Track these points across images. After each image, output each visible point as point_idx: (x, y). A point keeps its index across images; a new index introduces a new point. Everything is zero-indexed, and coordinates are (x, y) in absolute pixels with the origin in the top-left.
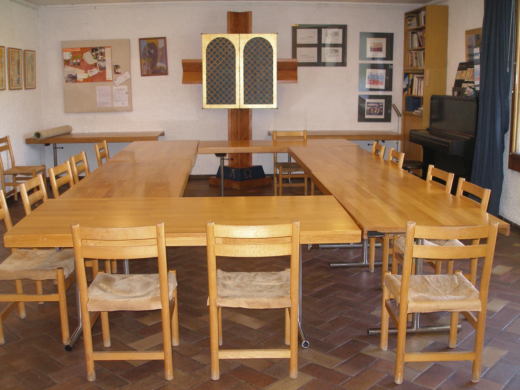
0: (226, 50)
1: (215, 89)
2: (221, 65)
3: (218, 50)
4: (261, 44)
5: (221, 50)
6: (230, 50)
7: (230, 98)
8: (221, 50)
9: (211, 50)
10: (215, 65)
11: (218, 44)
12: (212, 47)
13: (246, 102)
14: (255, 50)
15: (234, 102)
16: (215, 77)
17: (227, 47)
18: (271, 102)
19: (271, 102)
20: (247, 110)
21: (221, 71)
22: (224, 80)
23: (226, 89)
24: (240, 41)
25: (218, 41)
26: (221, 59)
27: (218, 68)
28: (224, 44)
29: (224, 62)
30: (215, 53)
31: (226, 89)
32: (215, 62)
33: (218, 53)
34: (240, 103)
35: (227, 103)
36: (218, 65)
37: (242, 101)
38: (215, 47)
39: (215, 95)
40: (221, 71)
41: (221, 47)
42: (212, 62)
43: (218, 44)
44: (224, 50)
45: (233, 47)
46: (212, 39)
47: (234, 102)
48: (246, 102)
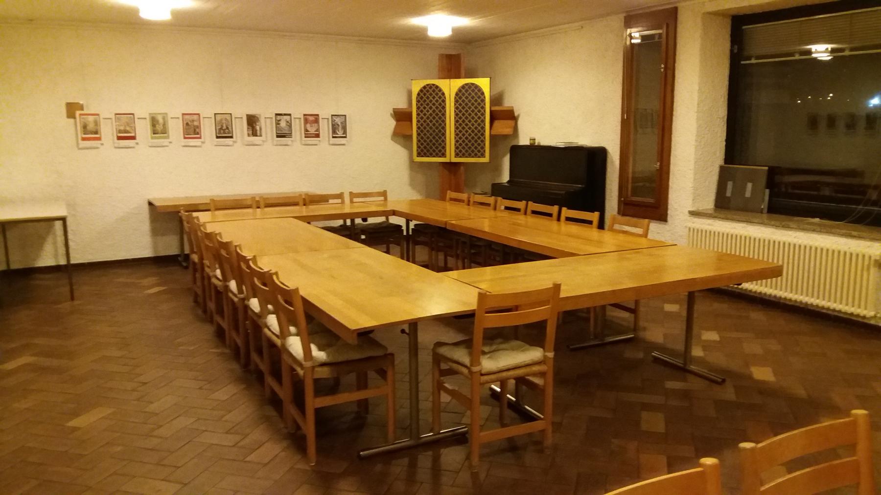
0: (437, 98)
1: (425, 141)
2: (431, 115)
3: (428, 98)
4: (473, 91)
5: (431, 98)
6: (440, 98)
7: (440, 151)
8: (431, 98)
9: (422, 98)
10: (425, 115)
11: (428, 91)
12: (422, 94)
13: (457, 155)
14: (467, 98)
15: (444, 155)
17: (437, 94)
19: (483, 155)
21: (431, 121)
26: (431, 108)
28: (434, 91)
30: (425, 101)
32: (425, 111)
33: (428, 101)
34: (451, 156)
35: (437, 155)
36: (428, 114)
37: (453, 154)
38: (425, 94)
41: (431, 94)
42: (422, 111)
43: (428, 91)
45: (443, 94)
47: (444, 155)
48: (457, 155)
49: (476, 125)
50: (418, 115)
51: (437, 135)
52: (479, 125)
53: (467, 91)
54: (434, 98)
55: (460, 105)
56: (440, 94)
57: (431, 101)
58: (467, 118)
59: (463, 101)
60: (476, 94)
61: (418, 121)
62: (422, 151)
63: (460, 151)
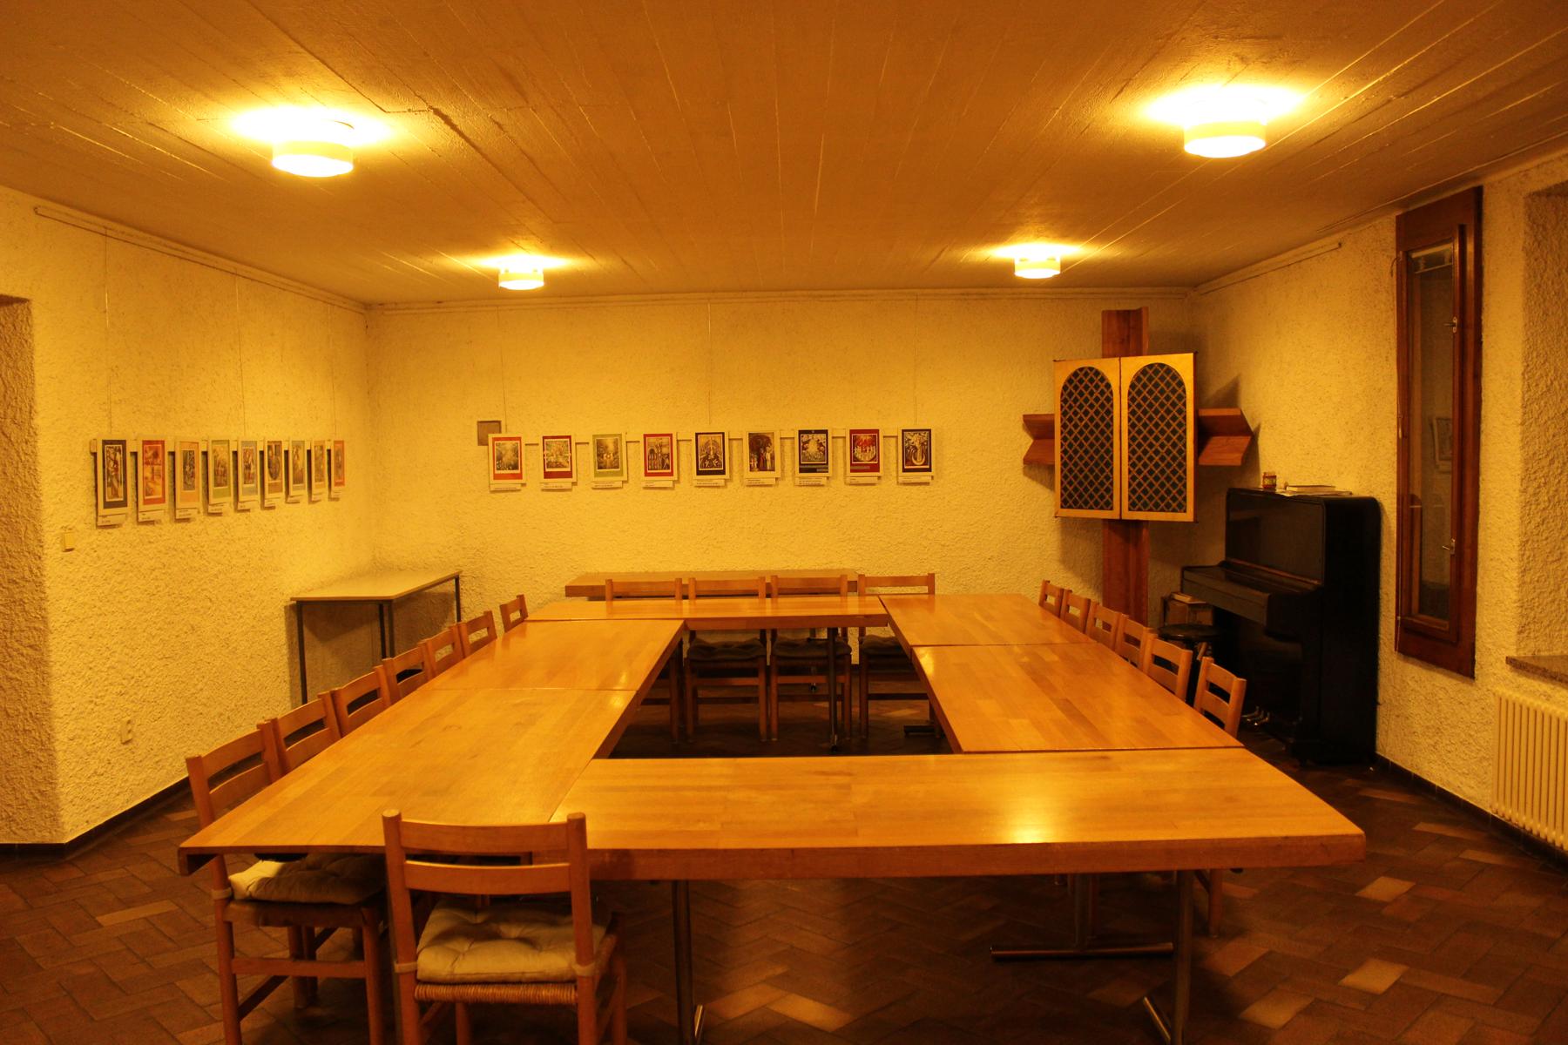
0: (1097, 394)
2: (1086, 426)
3: (1081, 394)
4: (1162, 379)
5: (1086, 394)
7: (1102, 497)
8: (1086, 394)
9: (1070, 394)
10: (1076, 426)
11: (1081, 381)
14: (1150, 392)
15: (1108, 505)
16: (1076, 452)
17: (1097, 387)
18: (1181, 508)
19: (1181, 508)
20: (1138, 523)
22: (1091, 458)
23: (1097, 477)
24: (1122, 372)
25: (1081, 375)
26: (1086, 413)
27: (1081, 433)
28: (1091, 381)
29: (1091, 419)
30: (1076, 400)
31: (1097, 477)
32: (1076, 419)
33: (1081, 401)
34: (1121, 508)
35: (1096, 506)
37: (1126, 503)
38: (1076, 388)
39: (1075, 489)
40: (1086, 439)
44: (1091, 393)
45: (1108, 386)
46: (1072, 370)
47: (1108, 505)
48: (1132, 506)
49: (1168, 446)
50: (1064, 426)
51: (1097, 465)
52: (1174, 445)
53: (1150, 379)
54: (1091, 393)
55: (1139, 406)
56: (1102, 386)
57: (1086, 400)
58: (1151, 432)
59: (1145, 399)
60: (1168, 385)
61: (1064, 439)
62: (1070, 496)
63: (1139, 498)
